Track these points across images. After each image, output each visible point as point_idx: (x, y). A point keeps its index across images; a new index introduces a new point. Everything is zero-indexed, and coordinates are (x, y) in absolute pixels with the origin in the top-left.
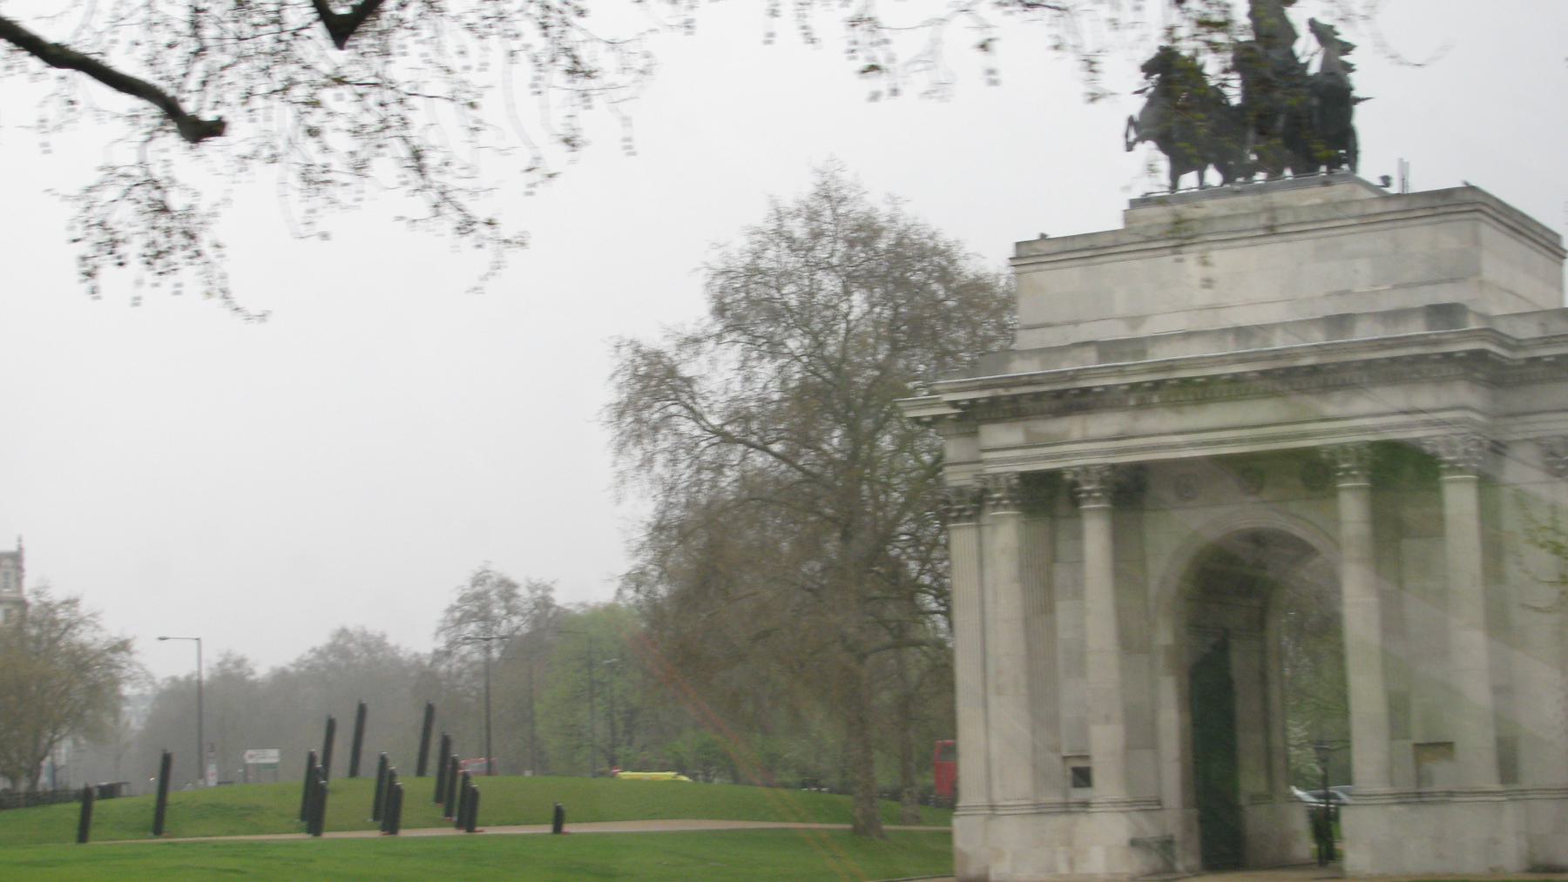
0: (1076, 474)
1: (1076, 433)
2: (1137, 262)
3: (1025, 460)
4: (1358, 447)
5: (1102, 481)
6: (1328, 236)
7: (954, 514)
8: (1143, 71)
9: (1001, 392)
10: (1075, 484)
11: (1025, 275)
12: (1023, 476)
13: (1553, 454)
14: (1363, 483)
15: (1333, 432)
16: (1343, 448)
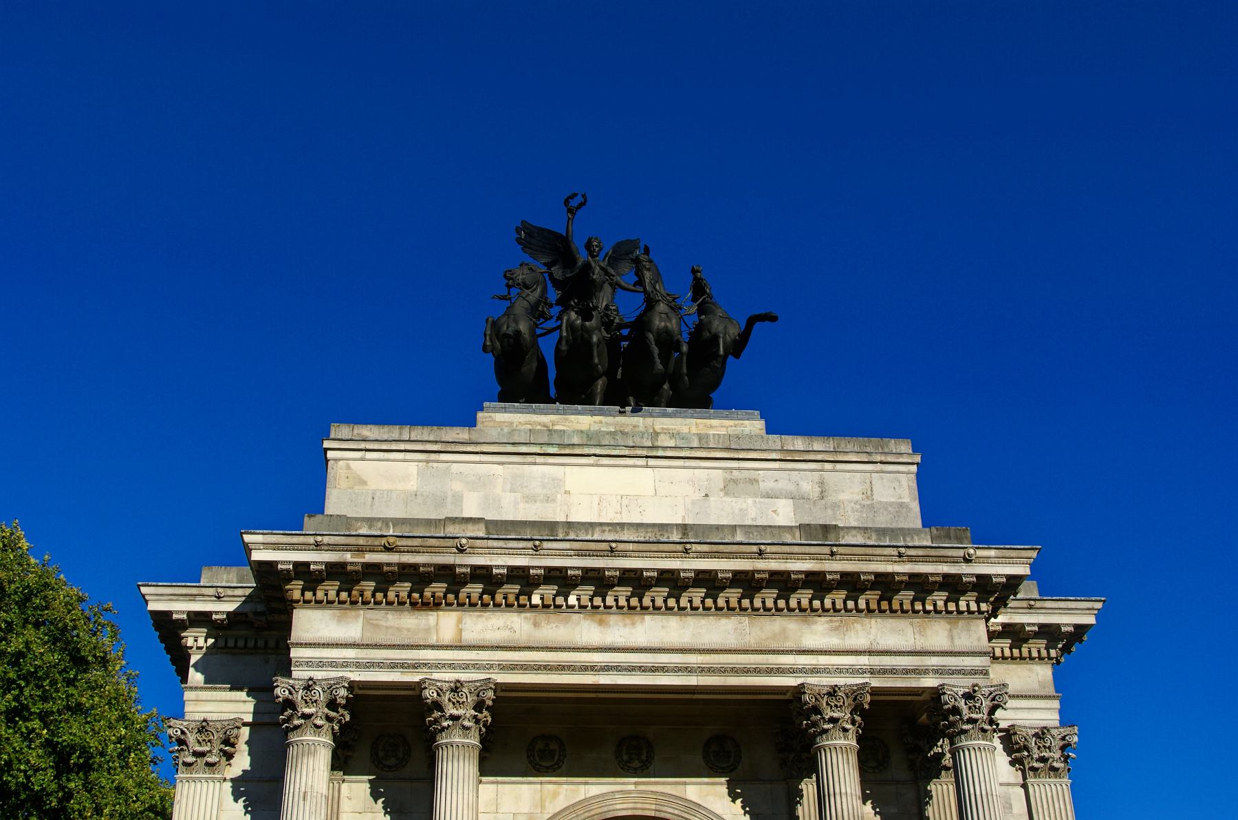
0: (440, 692)
1: (447, 636)
2: (500, 467)
3: (358, 665)
4: (855, 693)
5: (479, 706)
6: (739, 469)
7: (190, 759)
8: (505, 277)
9: (348, 557)
10: (438, 706)
11: (341, 463)
12: (352, 686)
13: (1026, 748)
14: (854, 743)
15: (815, 671)
16: (833, 692)
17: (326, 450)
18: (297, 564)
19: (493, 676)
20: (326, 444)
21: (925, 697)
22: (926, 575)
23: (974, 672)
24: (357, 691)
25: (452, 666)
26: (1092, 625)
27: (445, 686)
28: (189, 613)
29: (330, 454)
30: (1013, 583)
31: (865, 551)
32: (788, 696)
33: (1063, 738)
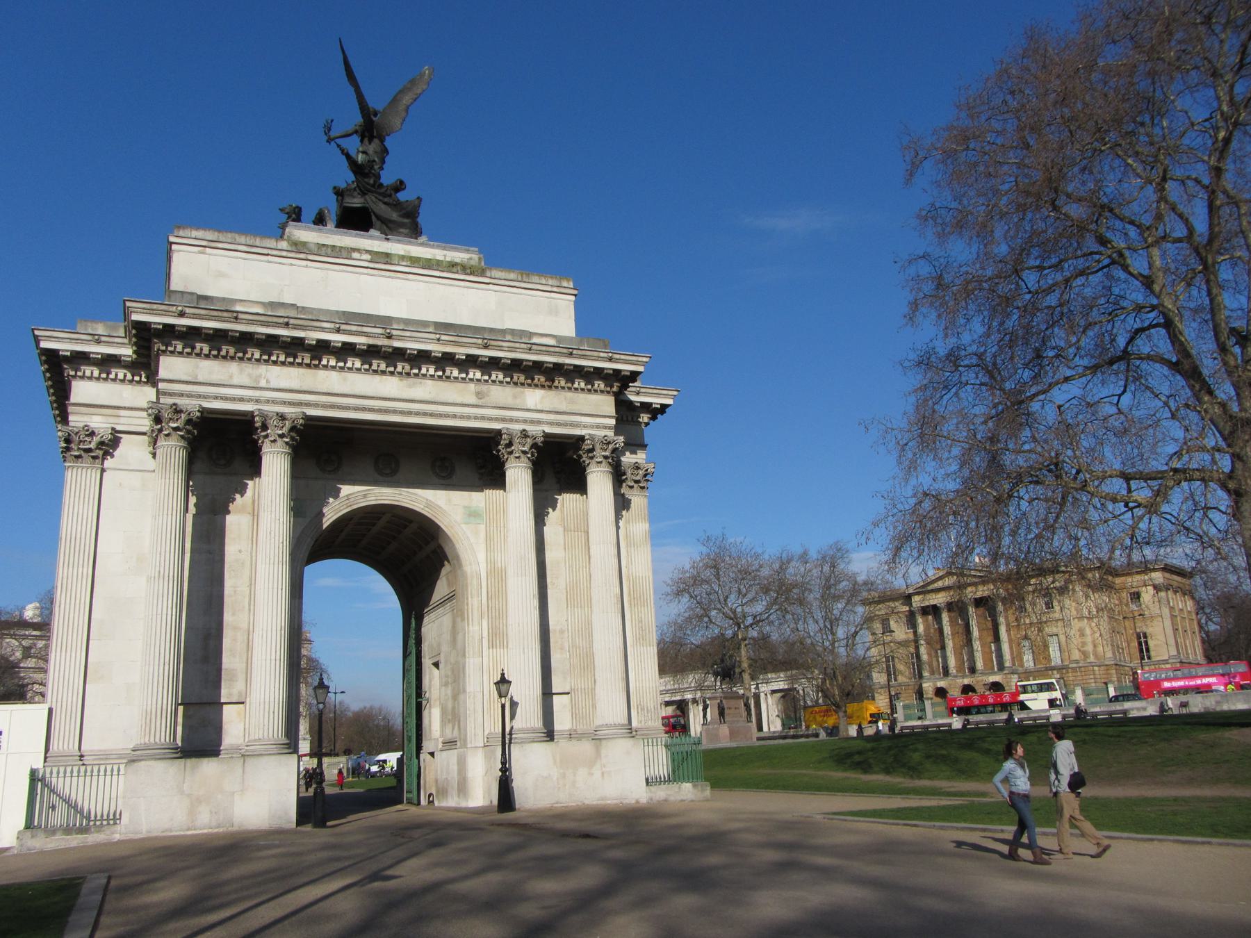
17: (171, 243)
18: (165, 325)
19: (305, 411)
20: (172, 239)
21: (573, 440)
22: (584, 367)
23: (605, 427)
24: (205, 414)
25: (274, 402)
26: (668, 406)
27: (270, 415)
28: (72, 352)
29: (174, 247)
30: (634, 376)
31: (546, 349)
32: (492, 435)
33: (647, 470)
